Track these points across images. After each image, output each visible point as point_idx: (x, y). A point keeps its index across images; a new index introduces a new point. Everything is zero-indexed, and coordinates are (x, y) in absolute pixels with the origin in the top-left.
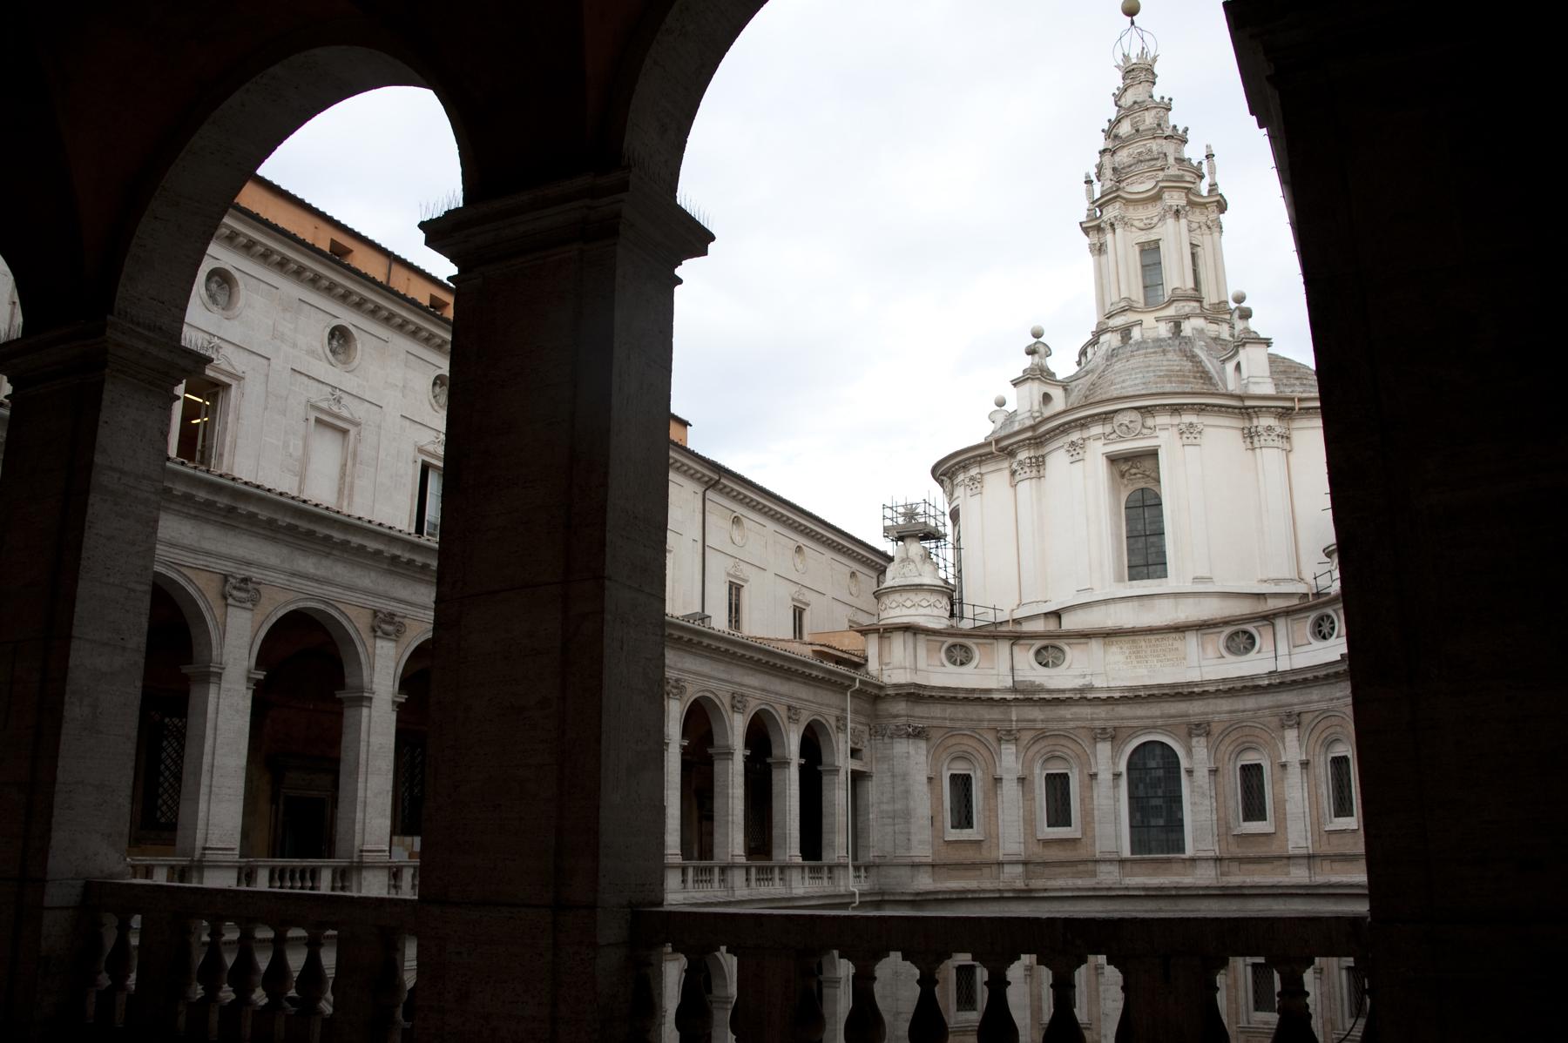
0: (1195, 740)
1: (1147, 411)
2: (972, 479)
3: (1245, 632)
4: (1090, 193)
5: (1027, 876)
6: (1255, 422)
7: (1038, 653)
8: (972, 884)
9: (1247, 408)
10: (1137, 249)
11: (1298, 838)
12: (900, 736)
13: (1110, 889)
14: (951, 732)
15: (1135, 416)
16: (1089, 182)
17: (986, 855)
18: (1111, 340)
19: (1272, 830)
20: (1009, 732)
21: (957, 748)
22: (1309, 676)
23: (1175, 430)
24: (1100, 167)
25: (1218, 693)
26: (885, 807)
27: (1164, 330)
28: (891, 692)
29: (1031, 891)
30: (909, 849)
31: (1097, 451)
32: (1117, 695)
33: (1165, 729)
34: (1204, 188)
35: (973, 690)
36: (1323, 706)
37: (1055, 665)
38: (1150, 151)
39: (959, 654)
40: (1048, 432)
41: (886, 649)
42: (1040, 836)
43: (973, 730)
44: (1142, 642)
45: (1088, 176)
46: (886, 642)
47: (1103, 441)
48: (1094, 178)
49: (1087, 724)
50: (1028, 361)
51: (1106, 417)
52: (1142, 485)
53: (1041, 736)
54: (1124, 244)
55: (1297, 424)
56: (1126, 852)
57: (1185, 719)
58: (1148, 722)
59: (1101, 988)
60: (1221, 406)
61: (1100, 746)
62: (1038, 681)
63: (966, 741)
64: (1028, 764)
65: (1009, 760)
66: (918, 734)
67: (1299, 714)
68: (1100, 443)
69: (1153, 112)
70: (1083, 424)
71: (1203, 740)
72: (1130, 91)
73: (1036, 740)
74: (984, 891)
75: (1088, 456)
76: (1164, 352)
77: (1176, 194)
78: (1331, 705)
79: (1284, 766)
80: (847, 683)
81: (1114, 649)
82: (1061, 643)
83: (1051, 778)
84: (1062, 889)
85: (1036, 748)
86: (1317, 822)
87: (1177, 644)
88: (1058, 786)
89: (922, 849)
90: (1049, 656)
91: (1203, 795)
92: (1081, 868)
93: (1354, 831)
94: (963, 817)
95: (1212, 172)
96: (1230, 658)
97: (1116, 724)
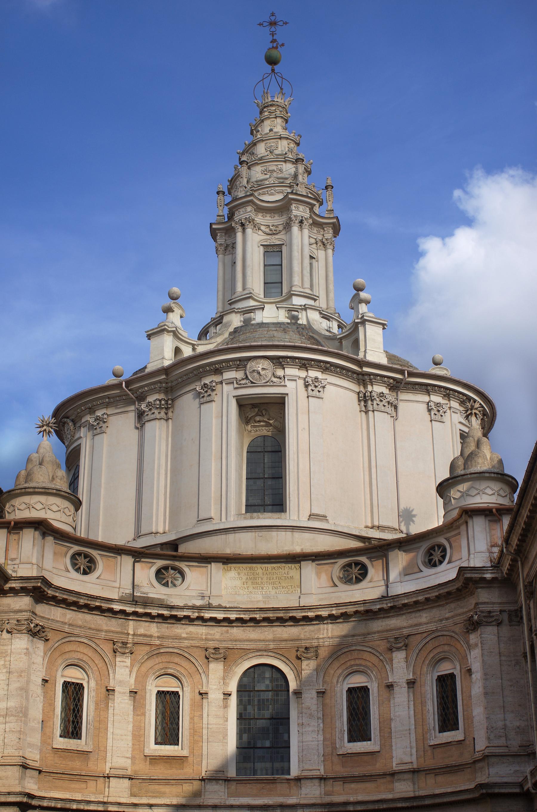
1: (279, 362)
2: (97, 419)
3: (357, 564)
6: (370, 388)
8: (78, 797)
9: (364, 374)
11: (403, 752)
12: (20, 631)
15: (266, 364)
19: (377, 748)
20: (125, 644)
21: (75, 655)
22: (421, 598)
23: (301, 383)
33: (277, 653)
36: (432, 627)
38: (281, 170)
41: (13, 544)
42: (147, 752)
43: (90, 639)
44: (259, 568)
46: (14, 537)
47: (236, 386)
49: (202, 644)
51: (241, 364)
53: (156, 652)
55: (403, 396)
56: (232, 773)
57: (297, 643)
58: (261, 645)
60: (343, 368)
61: (213, 666)
63: (82, 649)
64: (141, 679)
65: (123, 673)
66: (36, 632)
68: (231, 387)
69: (285, 142)
72: (267, 123)
74: (89, 802)
75: (217, 399)
76: (285, 331)
77: (301, 208)
78: (439, 625)
79: (390, 687)
81: (233, 574)
82: (183, 565)
85: (150, 664)
86: (421, 738)
88: (168, 702)
91: (311, 716)
96: (342, 587)
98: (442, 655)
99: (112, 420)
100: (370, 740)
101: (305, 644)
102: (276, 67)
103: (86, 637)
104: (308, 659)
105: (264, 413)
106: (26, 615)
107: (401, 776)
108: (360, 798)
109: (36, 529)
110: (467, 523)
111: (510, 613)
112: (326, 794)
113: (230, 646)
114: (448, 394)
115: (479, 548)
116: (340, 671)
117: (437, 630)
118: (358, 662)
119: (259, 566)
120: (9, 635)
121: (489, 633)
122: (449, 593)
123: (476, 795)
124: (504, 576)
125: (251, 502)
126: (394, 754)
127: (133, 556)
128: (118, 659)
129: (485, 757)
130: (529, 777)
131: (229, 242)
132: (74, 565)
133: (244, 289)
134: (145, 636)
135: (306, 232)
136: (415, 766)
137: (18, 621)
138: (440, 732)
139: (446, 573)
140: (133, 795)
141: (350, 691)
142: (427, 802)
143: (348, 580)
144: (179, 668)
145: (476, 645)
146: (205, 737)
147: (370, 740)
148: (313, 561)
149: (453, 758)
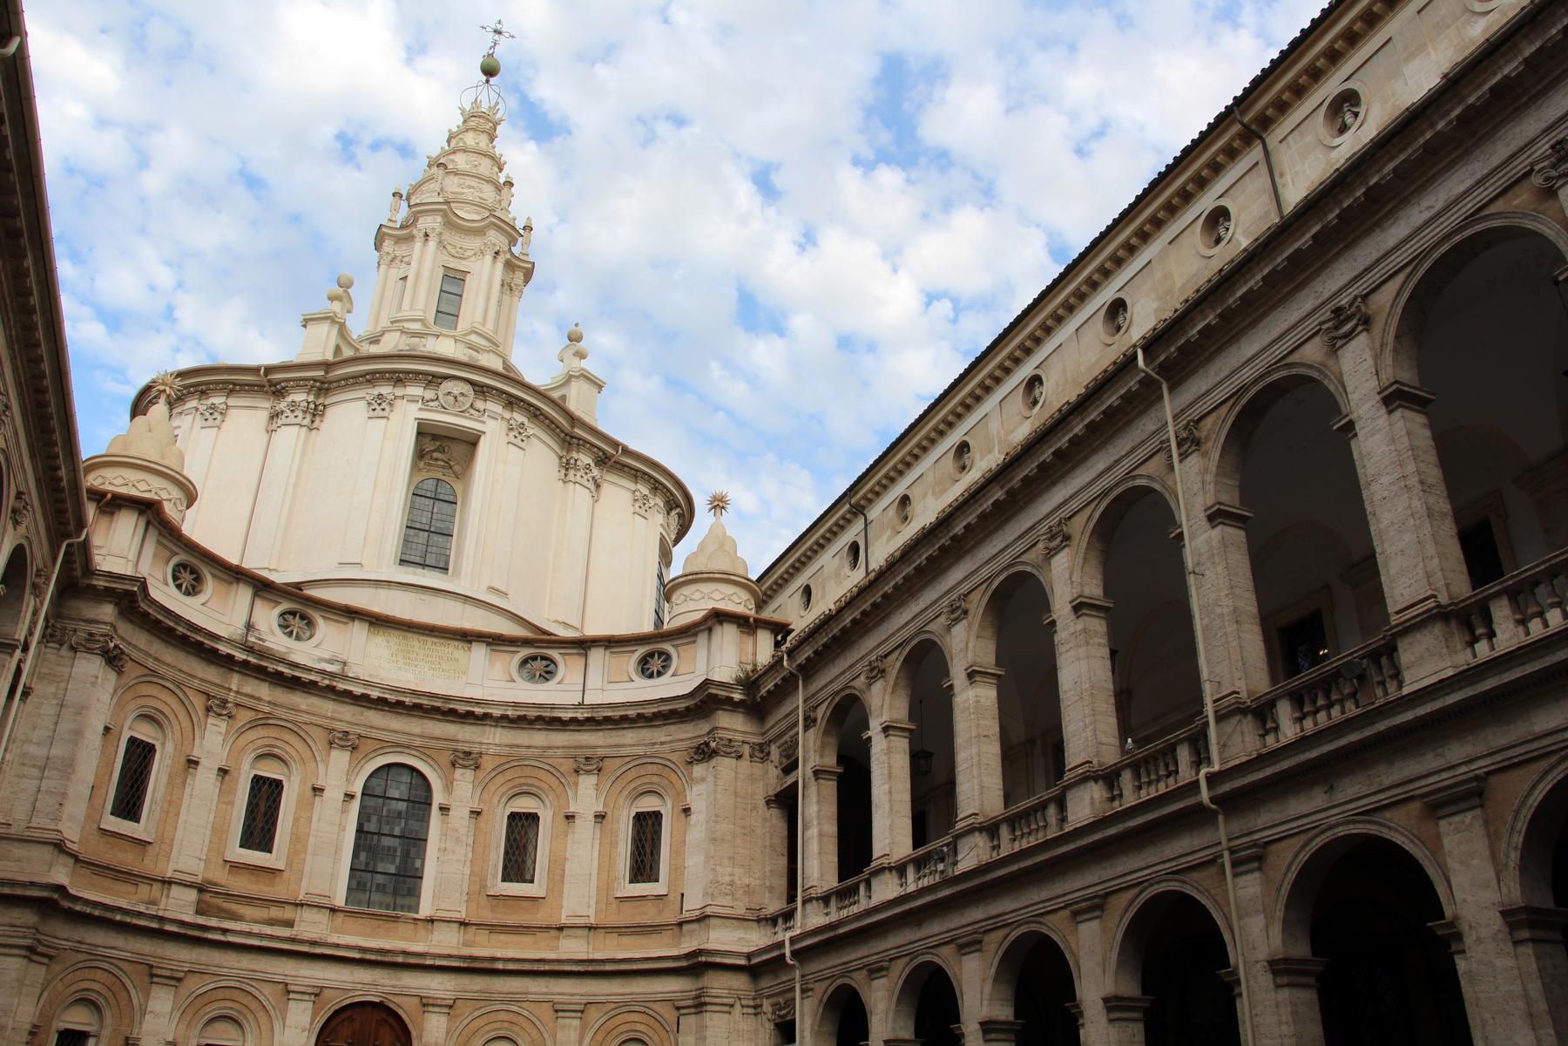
0: (459, 772)
1: (481, 390)
2: (213, 407)
3: (544, 658)
5: (199, 912)
7: (282, 615)
10: (441, 272)
12: (90, 651)
13: (314, 943)
14: (151, 675)
15: (467, 389)
20: (225, 702)
22: (632, 713)
25: (506, 721)
26: (32, 749)
28: (101, 583)
30: (58, 819)
32: (375, 694)
33: (423, 751)
36: (640, 750)
37: (298, 638)
47: (420, 405)
51: (434, 380)
54: (426, 260)
56: (340, 900)
63: (165, 696)
65: (213, 741)
66: (113, 659)
67: (602, 759)
70: (399, 378)
71: (469, 774)
73: (254, 725)
74: (140, 914)
78: (649, 750)
79: (570, 818)
80: (72, 527)
83: (258, 781)
84: (249, 934)
85: (252, 735)
89: (72, 833)
90: (296, 622)
92: (275, 912)
95: (528, 243)
98: (648, 788)
99: (232, 412)
100: (532, 881)
101: (460, 747)
102: (492, 80)
103: (173, 682)
104: (465, 767)
105: (444, 451)
106: (106, 629)
107: (572, 932)
109: (141, 513)
110: (710, 630)
112: (465, 944)
113: (363, 733)
114: (656, 487)
115: (725, 659)
116: (504, 789)
117: (645, 756)
118: (529, 781)
119: (416, 637)
120: (71, 654)
121: (725, 765)
122: (673, 713)
123: (684, 963)
124: (758, 697)
125: (407, 558)
126: (565, 903)
127: (255, 586)
128: (211, 720)
129: (702, 918)
130: (787, 944)
132: (175, 578)
133: (411, 309)
134: (252, 697)
136: (592, 921)
137: (91, 634)
138: (631, 882)
139: (675, 685)
140: (199, 912)
141: (513, 817)
142: (609, 967)
143: (532, 678)
144: (288, 748)
145: (703, 779)
146: (310, 847)
147: (532, 881)
148: (489, 644)
149: (649, 915)
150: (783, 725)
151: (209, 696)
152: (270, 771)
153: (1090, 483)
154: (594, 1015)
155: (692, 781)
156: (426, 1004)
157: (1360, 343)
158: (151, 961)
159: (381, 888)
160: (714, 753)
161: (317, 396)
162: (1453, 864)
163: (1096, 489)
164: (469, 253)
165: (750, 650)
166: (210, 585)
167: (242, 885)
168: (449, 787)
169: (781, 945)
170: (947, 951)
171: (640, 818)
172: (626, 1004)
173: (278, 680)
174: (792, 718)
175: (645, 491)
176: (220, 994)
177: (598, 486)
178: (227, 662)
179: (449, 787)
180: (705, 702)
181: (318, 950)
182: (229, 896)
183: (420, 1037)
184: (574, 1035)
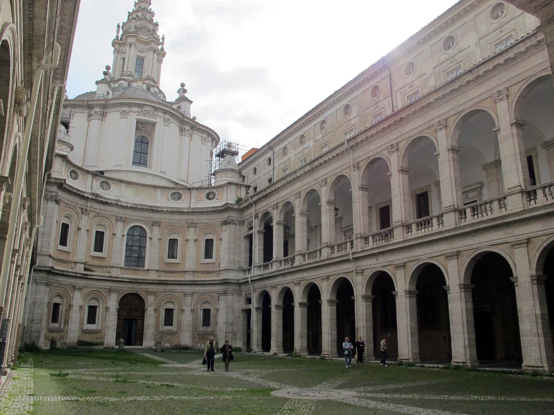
0: (154, 227)
4: (118, 32)
5: (85, 269)
7: (101, 183)
8: (65, 269)
12: (52, 200)
13: (117, 278)
15: (152, 109)
16: (118, 27)
17: (71, 258)
18: (126, 84)
19: (179, 262)
20: (87, 210)
22: (205, 210)
23: (162, 119)
24: (124, 24)
27: (145, 87)
29: (87, 275)
30: (49, 249)
31: (133, 117)
32: (129, 206)
33: (143, 222)
34: (160, 47)
35: (79, 190)
36: (207, 221)
38: (148, 27)
39: (74, 175)
40: (113, 104)
45: (119, 24)
48: (121, 25)
49: (116, 215)
50: (103, 77)
51: (140, 106)
52: (143, 135)
53: (98, 215)
54: (131, 54)
55: (194, 132)
56: (123, 265)
57: (152, 220)
59: (107, 316)
62: (100, 194)
63: (71, 210)
65: (85, 222)
66: (57, 202)
67: (196, 223)
69: (150, 15)
70: (130, 105)
71: (157, 228)
73: (95, 216)
79: (187, 240)
81: (129, 189)
82: (110, 182)
84: (99, 276)
85: (95, 219)
87: (153, 192)
88: (100, 236)
89: (52, 252)
90: (105, 186)
92: (105, 269)
93: (213, 263)
94: (63, 242)
97: (126, 216)
99: (76, 114)
100: (176, 258)
101: (154, 220)
106: (55, 194)
108: (171, 279)
111: (240, 222)
112: (158, 276)
114: (209, 135)
128: (84, 216)
131: (121, 49)
132: (71, 175)
135: (156, 55)
142: (199, 283)
143: (174, 199)
145: (226, 231)
147: (176, 258)
150: (249, 216)
151: (82, 209)
152: (100, 229)
153: (332, 171)
154: (195, 296)
155: (222, 231)
156: (148, 293)
157: (395, 154)
158: (74, 284)
159: (134, 261)
160: (229, 223)
161: (103, 109)
162: (398, 280)
163: (334, 173)
164: (145, 50)
165: (239, 193)
166: (80, 176)
167: (96, 262)
168: (151, 231)
169: (248, 278)
170: (291, 284)
171: (207, 241)
172: (204, 292)
173: (102, 203)
174: (251, 215)
175: (206, 136)
176: (92, 292)
177: (191, 135)
178: (87, 199)
179: (151, 231)
180: (227, 208)
181: (118, 279)
182: (92, 265)
183: (147, 302)
184: (190, 301)
